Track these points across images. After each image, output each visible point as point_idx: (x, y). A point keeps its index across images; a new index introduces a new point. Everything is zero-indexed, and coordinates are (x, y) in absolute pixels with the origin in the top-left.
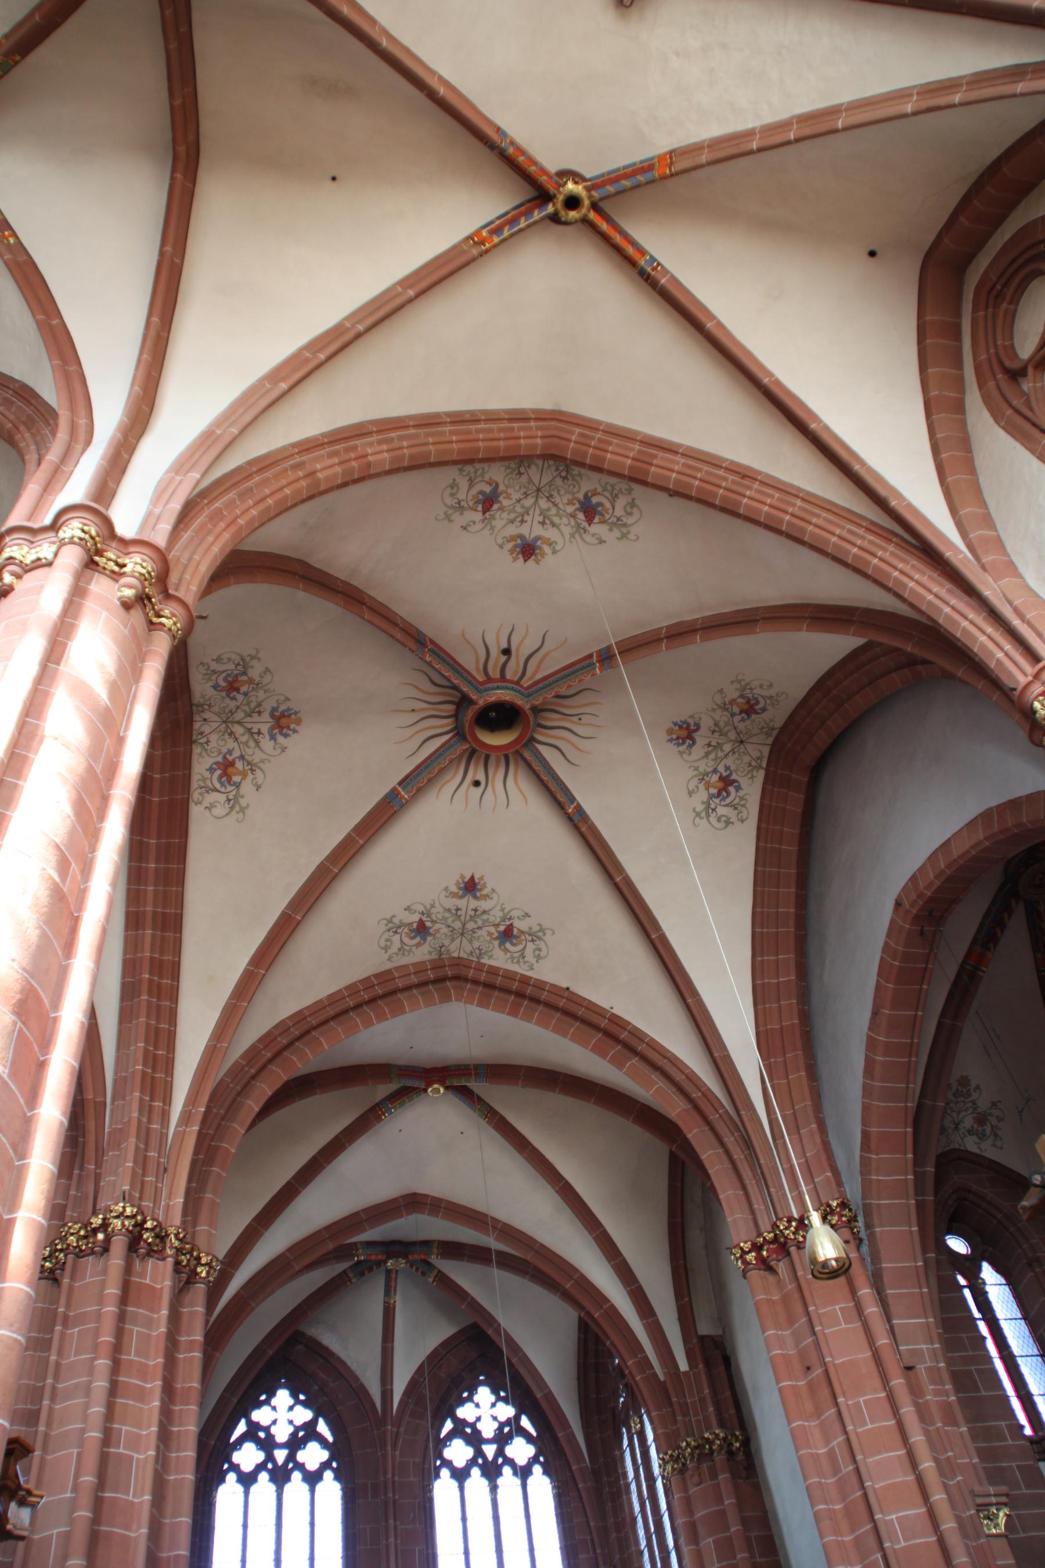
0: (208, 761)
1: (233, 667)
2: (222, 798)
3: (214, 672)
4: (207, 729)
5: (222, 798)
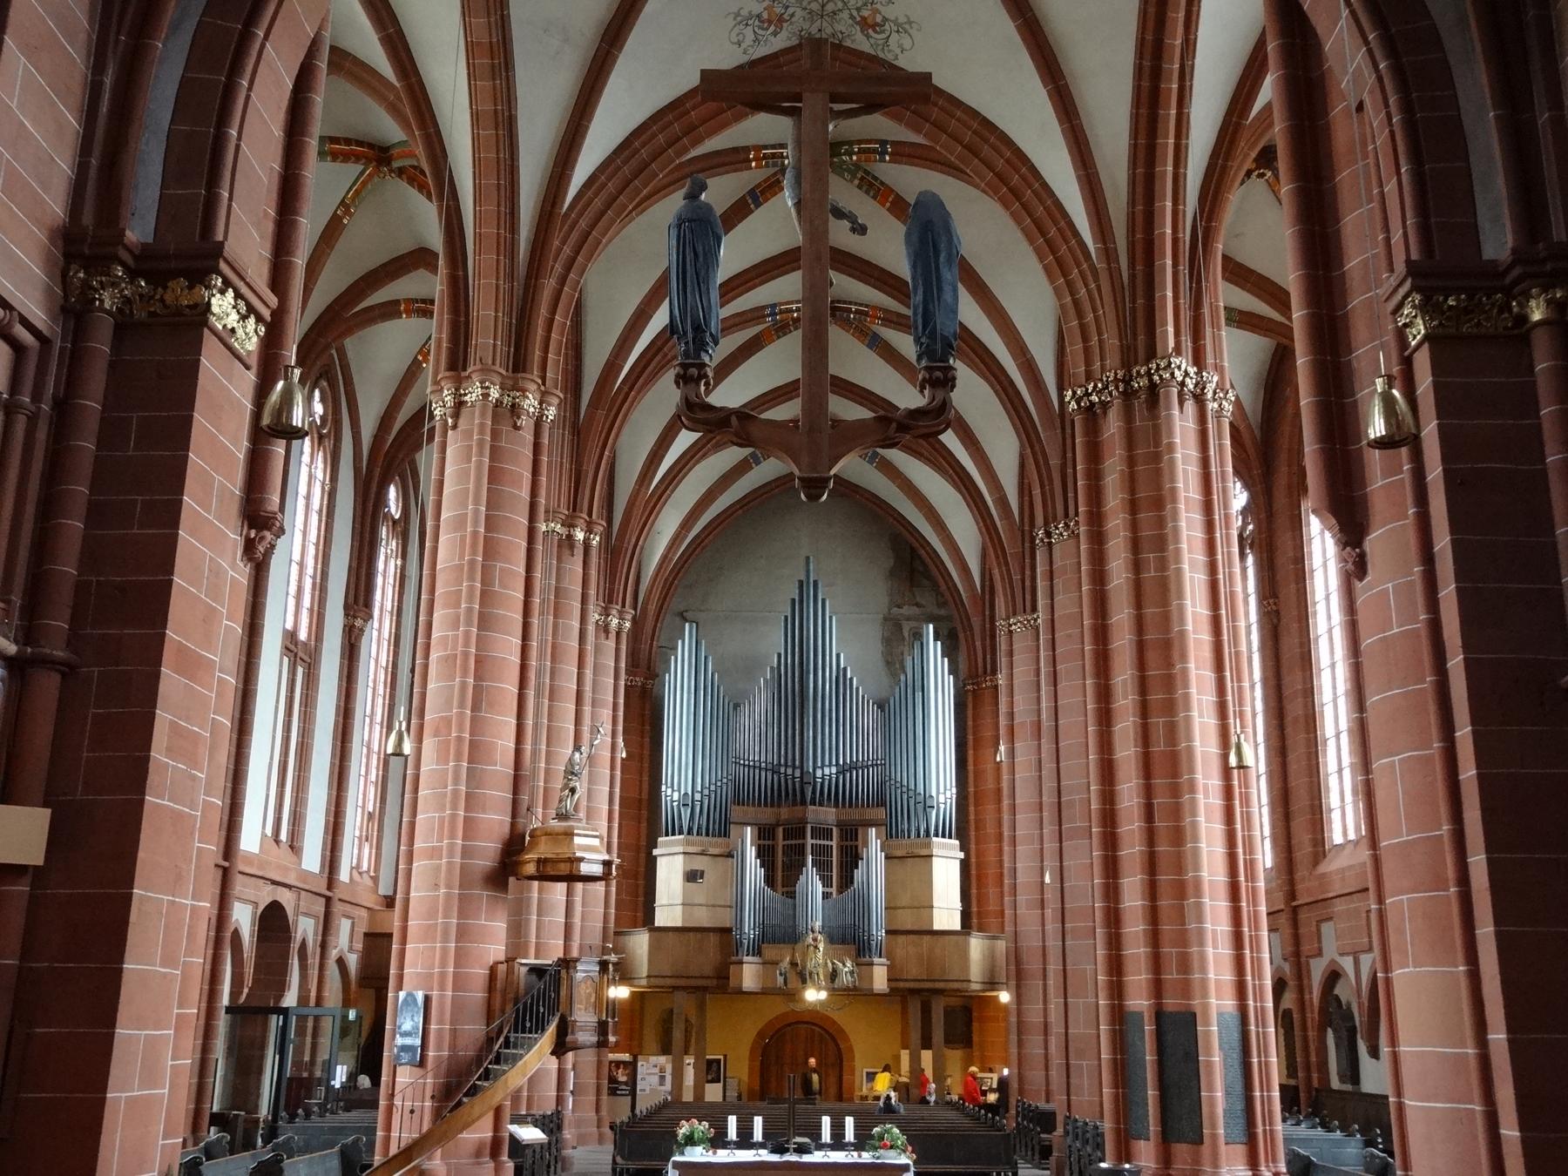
0: (859, 36)
1: (750, 28)
2: (894, 36)
3: (756, 40)
4: (829, 31)
5: (894, 35)
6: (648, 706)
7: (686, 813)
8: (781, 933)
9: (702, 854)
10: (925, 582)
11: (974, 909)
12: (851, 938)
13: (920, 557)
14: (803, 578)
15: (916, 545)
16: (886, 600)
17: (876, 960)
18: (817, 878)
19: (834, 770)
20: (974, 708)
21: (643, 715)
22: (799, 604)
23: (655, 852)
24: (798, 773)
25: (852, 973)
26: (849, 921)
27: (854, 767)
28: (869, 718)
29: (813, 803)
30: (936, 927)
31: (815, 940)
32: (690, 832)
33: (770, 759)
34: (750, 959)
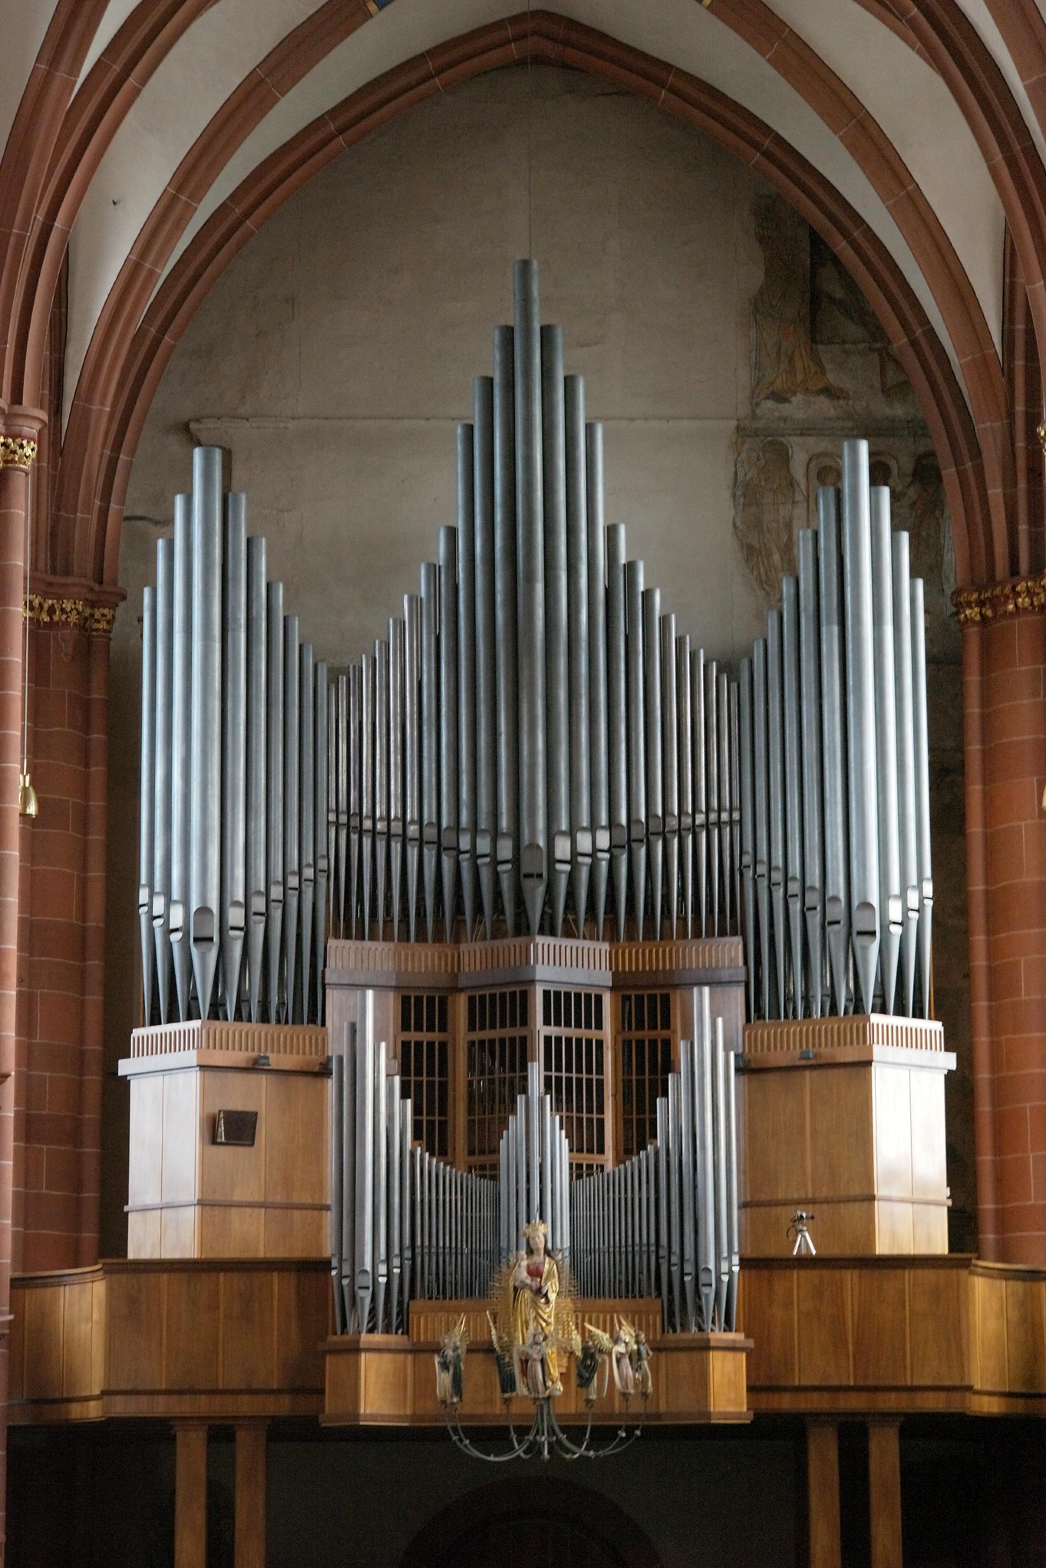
6: (98, 677)
7: (205, 961)
8: (455, 1269)
9: (255, 1067)
10: (853, 330)
11: (988, 1205)
12: (641, 1273)
13: (836, 261)
14: (513, 319)
18: (553, 1121)
20: (986, 668)
21: (87, 707)
23: (124, 1067)
24: (505, 850)
25: (635, 1358)
27: (656, 830)
28: (697, 703)
29: (549, 928)
30: (883, 1247)
31: (535, 1272)
32: (216, 1011)
33: (429, 814)
34: (378, 1338)
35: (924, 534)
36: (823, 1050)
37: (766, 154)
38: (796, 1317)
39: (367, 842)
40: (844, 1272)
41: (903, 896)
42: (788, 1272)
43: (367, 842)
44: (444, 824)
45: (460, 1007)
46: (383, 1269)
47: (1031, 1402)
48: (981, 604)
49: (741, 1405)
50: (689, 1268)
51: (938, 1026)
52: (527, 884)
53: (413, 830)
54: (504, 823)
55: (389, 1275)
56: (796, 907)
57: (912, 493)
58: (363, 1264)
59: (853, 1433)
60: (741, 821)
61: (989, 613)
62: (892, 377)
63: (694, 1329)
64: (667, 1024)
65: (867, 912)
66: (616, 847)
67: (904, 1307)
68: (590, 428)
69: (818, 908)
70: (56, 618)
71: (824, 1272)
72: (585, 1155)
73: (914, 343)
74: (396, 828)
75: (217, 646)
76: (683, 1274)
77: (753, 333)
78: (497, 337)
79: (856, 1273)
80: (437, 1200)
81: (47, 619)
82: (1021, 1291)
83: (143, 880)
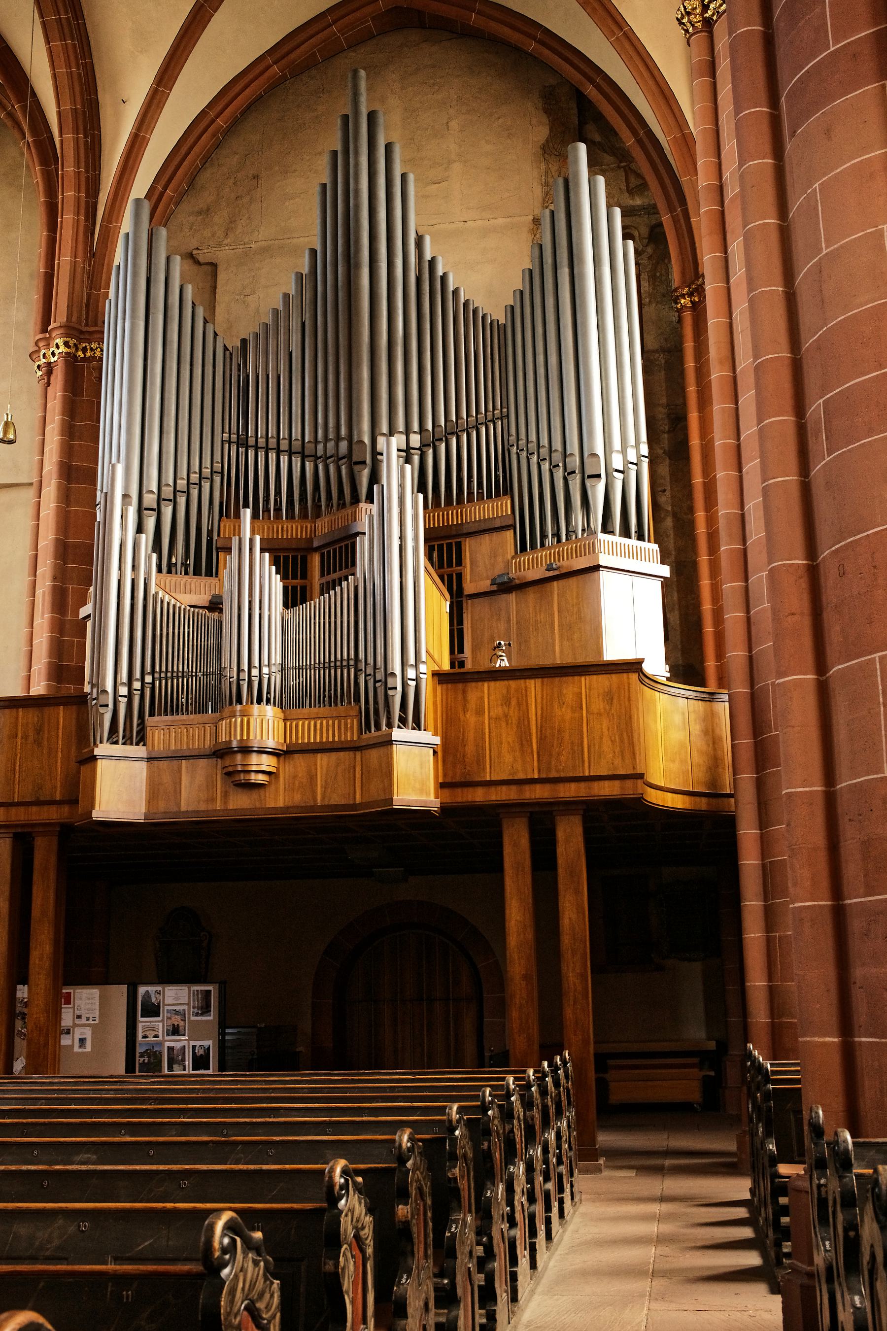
14: (348, 111)
15: (575, 77)
16: (538, 191)
17: (397, 734)
19: (415, 440)
22: (342, 162)
26: (346, 652)
27: (453, 431)
33: (296, 433)
35: (658, 274)
36: (565, 563)
37: (540, 42)
38: (487, 722)
39: (251, 453)
40: (527, 680)
41: (624, 451)
42: (480, 684)
43: (251, 453)
44: (307, 440)
45: (316, 560)
46: (123, 690)
47: (714, 801)
48: (690, 294)
49: (428, 794)
50: (380, 676)
51: (655, 547)
52: (356, 468)
53: (284, 445)
54: (343, 431)
55: (130, 696)
56: (546, 466)
57: (650, 250)
58: (104, 685)
59: (542, 821)
60: (508, 416)
61: (697, 299)
62: (634, 182)
63: (384, 728)
64: (459, 563)
65: (594, 459)
66: (424, 446)
67: (581, 708)
68: (404, 177)
69: (561, 465)
70: (88, 354)
71: (511, 682)
72: (290, 581)
73: (639, 141)
74: (273, 443)
75: (142, 324)
76: (375, 682)
77: (543, 166)
78: (339, 121)
79: (539, 681)
80: (173, 633)
81: (82, 355)
82: (701, 709)
83: (99, 488)
